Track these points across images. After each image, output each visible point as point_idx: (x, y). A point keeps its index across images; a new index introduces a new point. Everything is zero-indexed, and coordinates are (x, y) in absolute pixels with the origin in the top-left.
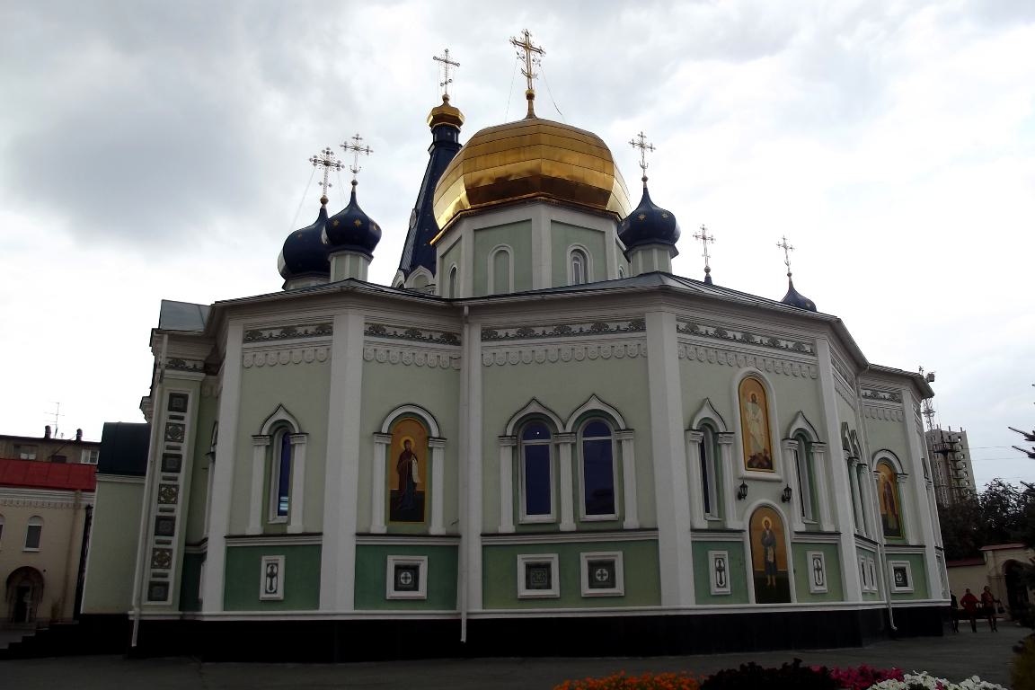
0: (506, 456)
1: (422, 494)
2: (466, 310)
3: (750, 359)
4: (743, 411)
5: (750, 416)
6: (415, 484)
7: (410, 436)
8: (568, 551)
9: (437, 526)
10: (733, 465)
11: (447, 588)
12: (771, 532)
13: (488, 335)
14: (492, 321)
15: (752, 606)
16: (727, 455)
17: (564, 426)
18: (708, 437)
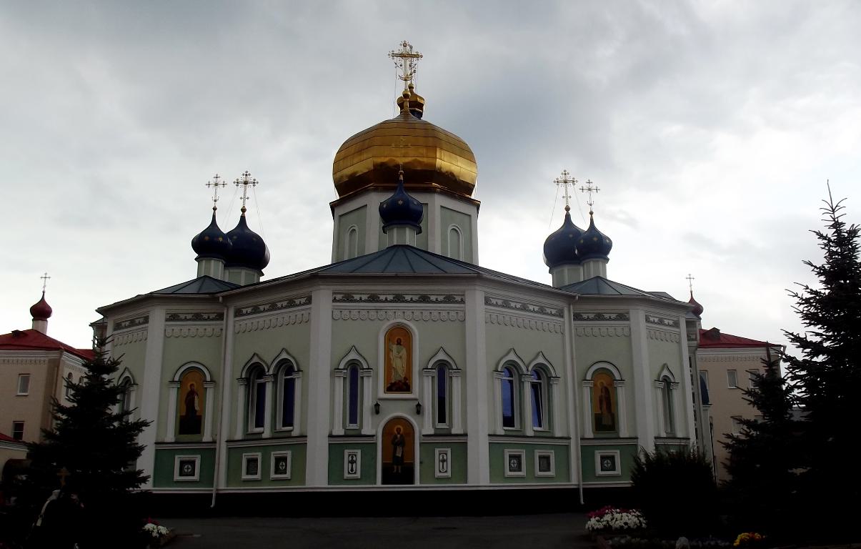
1: (201, 416)
2: (221, 299)
4: (388, 351)
6: (196, 411)
8: (265, 450)
9: (207, 437)
10: (373, 389)
11: (208, 477)
12: (402, 436)
13: (238, 313)
14: (240, 304)
15: (379, 485)
17: (268, 371)
18: (354, 373)
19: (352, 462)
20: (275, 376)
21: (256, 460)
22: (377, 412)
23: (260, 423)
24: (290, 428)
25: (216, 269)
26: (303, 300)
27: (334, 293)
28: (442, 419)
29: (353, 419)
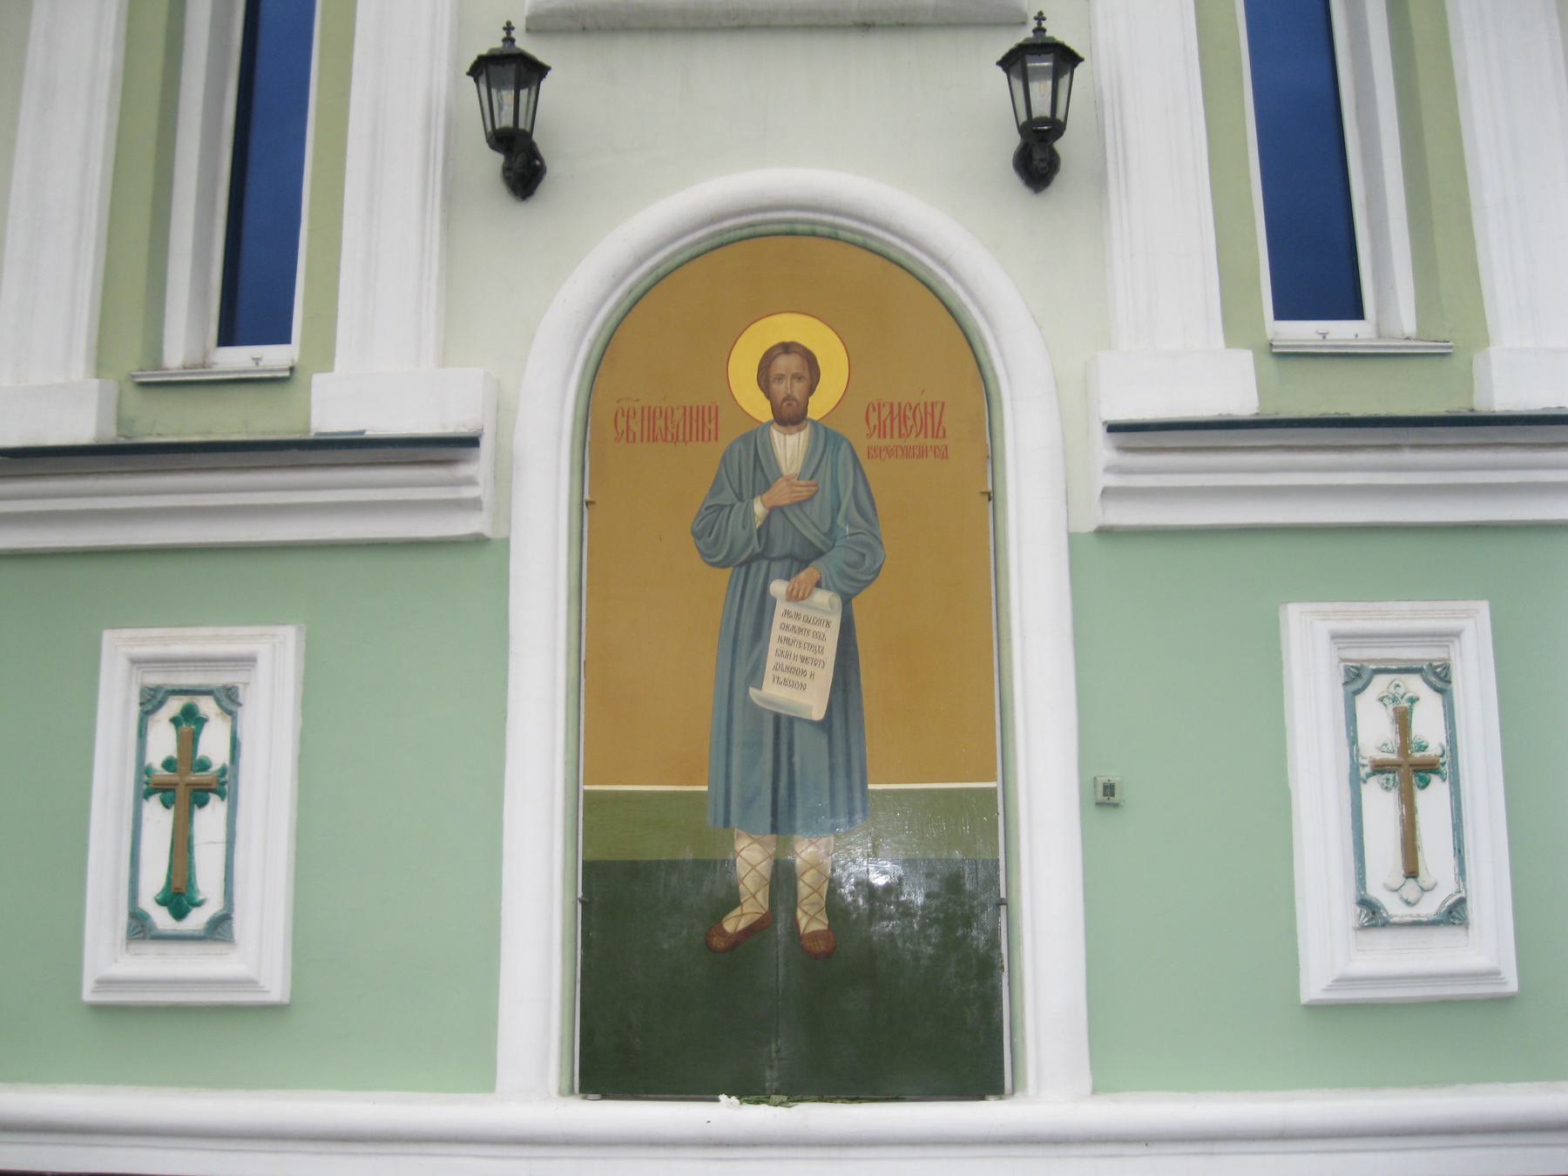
12: (827, 440)
19: (187, 787)
22: (523, 166)
28: (1313, 261)
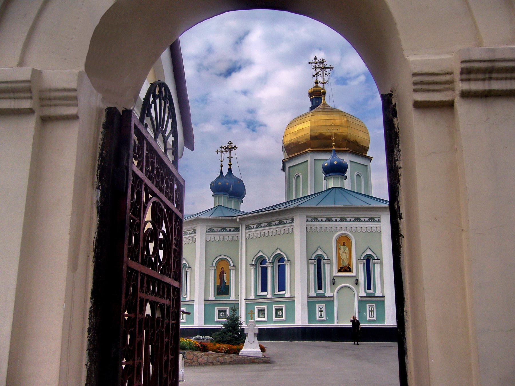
0: (252, 271)
2: (238, 220)
3: (343, 228)
4: (338, 249)
5: (341, 251)
7: (222, 265)
9: (232, 297)
10: (330, 271)
13: (248, 227)
14: (249, 222)
16: (327, 268)
19: (321, 311)
20: (273, 263)
21: (264, 310)
22: (334, 284)
23: (264, 289)
24: (284, 292)
25: (223, 201)
26: (288, 221)
27: (307, 217)
28: (369, 288)
29: (320, 288)
